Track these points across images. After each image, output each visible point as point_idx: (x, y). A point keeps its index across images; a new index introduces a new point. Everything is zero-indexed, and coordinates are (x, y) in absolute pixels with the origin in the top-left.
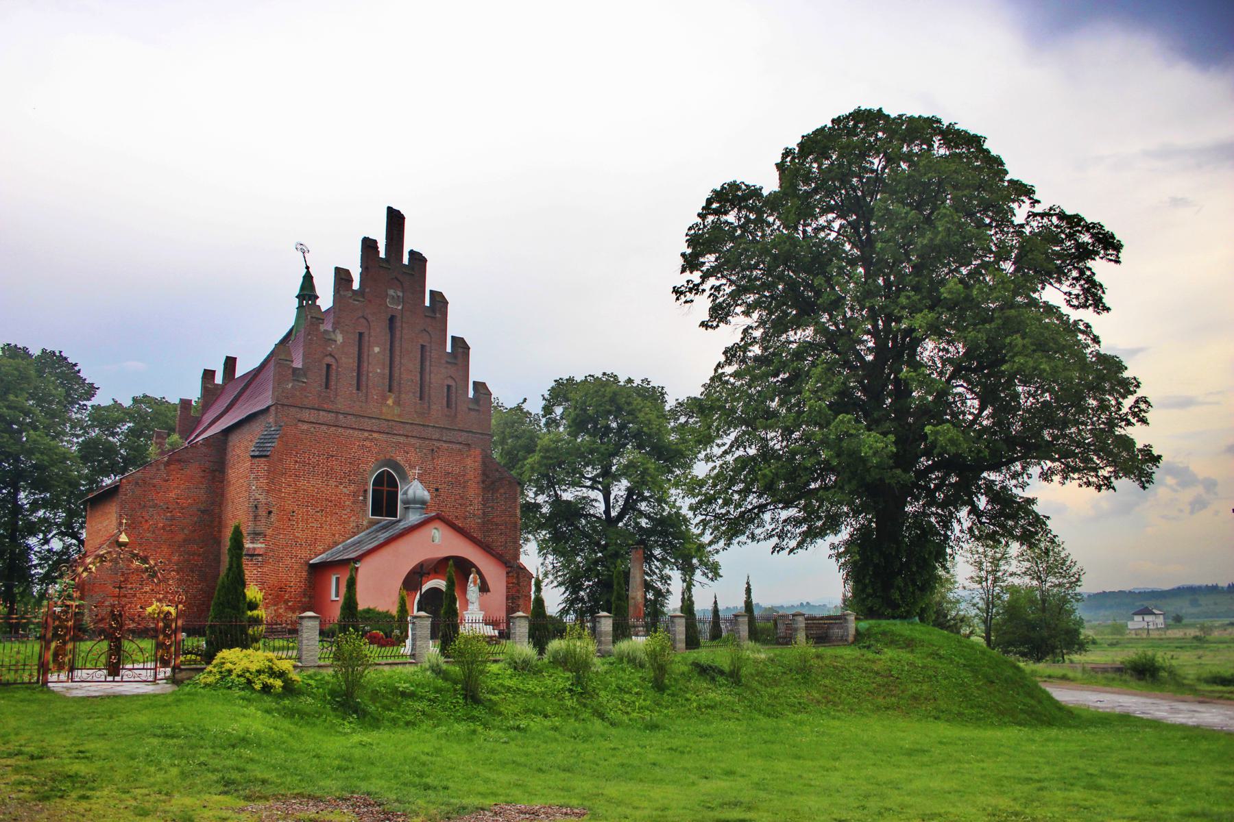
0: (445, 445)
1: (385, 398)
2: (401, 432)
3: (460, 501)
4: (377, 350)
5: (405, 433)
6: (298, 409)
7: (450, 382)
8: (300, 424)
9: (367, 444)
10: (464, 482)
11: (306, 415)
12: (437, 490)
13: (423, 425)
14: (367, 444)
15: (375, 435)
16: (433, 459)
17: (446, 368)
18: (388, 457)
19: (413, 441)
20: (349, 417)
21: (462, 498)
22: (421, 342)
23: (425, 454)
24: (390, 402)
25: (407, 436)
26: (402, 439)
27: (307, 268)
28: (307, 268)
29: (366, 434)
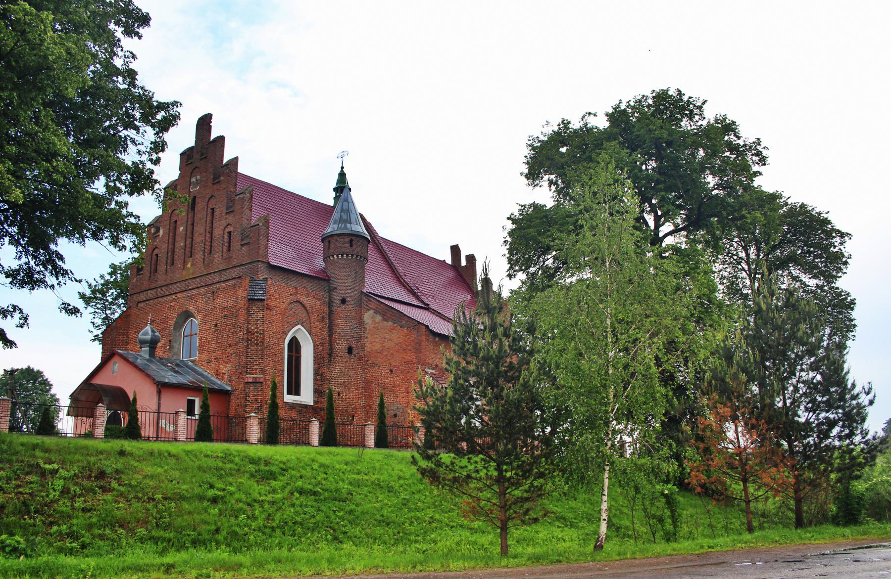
0: (223, 285)
1: (185, 263)
2: (193, 286)
3: (232, 331)
4: (181, 229)
5: (197, 286)
6: (138, 295)
7: (230, 229)
8: (139, 305)
9: (173, 304)
10: (236, 312)
11: (142, 297)
12: (216, 325)
13: (207, 274)
14: (173, 304)
15: (179, 295)
16: (214, 300)
17: (226, 218)
18: (184, 309)
19: (202, 290)
20: (163, 288)
21: (234, 327)
22: (210, 206)
23: (209, 298)
24: (189, 266)
25: (198, 288)
26: (195, 292)
27: (342, 168)
28: (342, 168)
29: (173, 297)
